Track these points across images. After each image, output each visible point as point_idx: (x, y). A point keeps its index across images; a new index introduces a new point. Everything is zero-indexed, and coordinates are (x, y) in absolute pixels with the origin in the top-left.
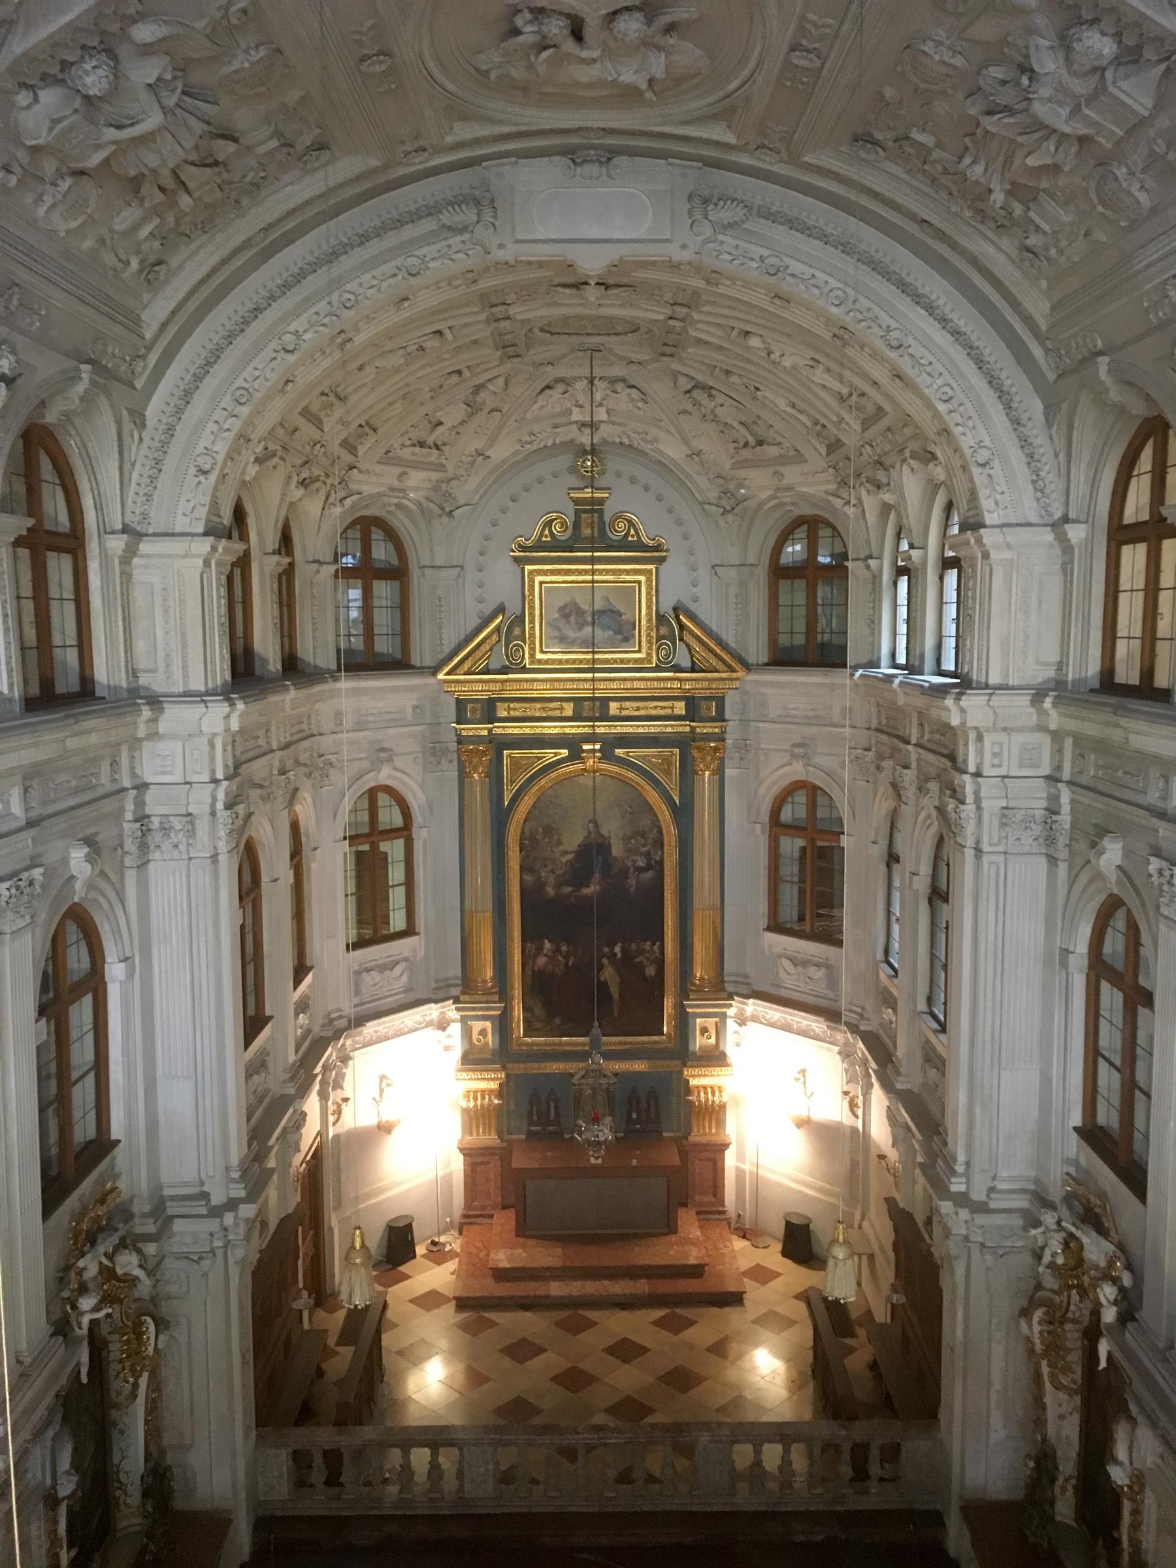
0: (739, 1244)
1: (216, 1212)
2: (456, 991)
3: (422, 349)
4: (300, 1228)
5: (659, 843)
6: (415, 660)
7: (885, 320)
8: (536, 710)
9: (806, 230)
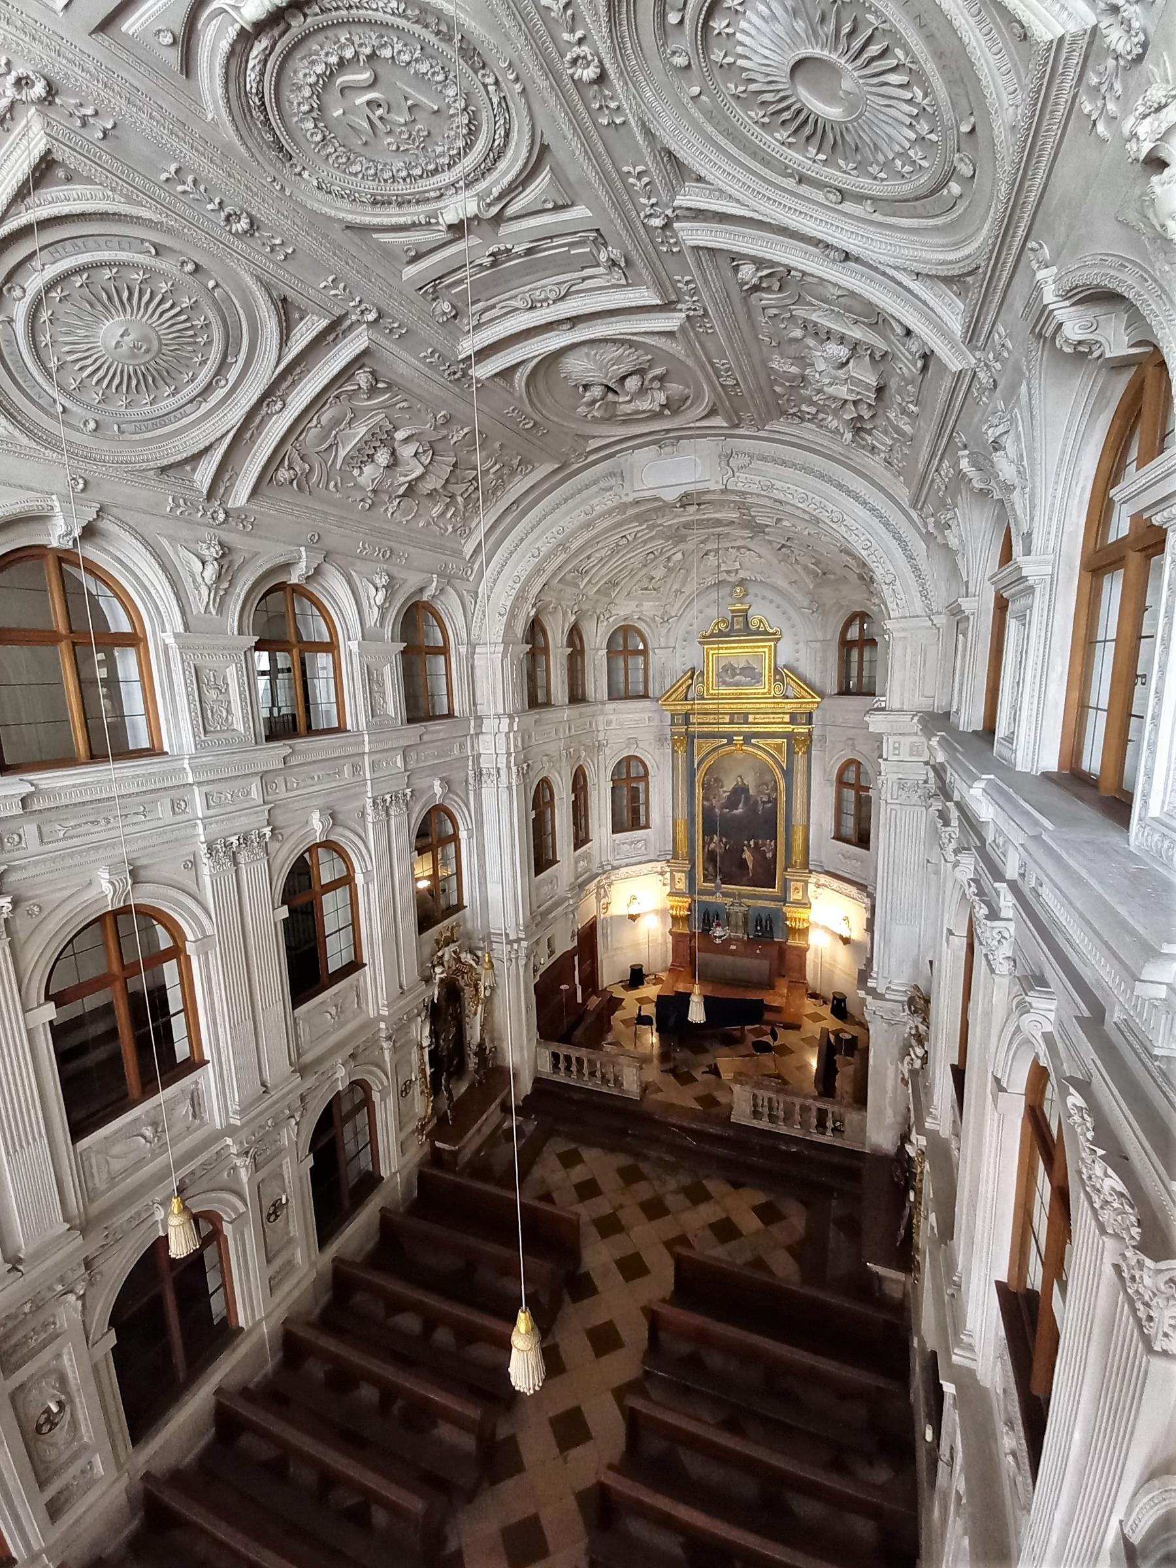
0: (809, 1002)
1: (510, 942)
2: (669, 857)
3: (618, 545)
4: (576, 958)
5: (775, 789)
6: (651, 695)
7: (830, 507)
8: (711, 719)
9: (783, 463)
